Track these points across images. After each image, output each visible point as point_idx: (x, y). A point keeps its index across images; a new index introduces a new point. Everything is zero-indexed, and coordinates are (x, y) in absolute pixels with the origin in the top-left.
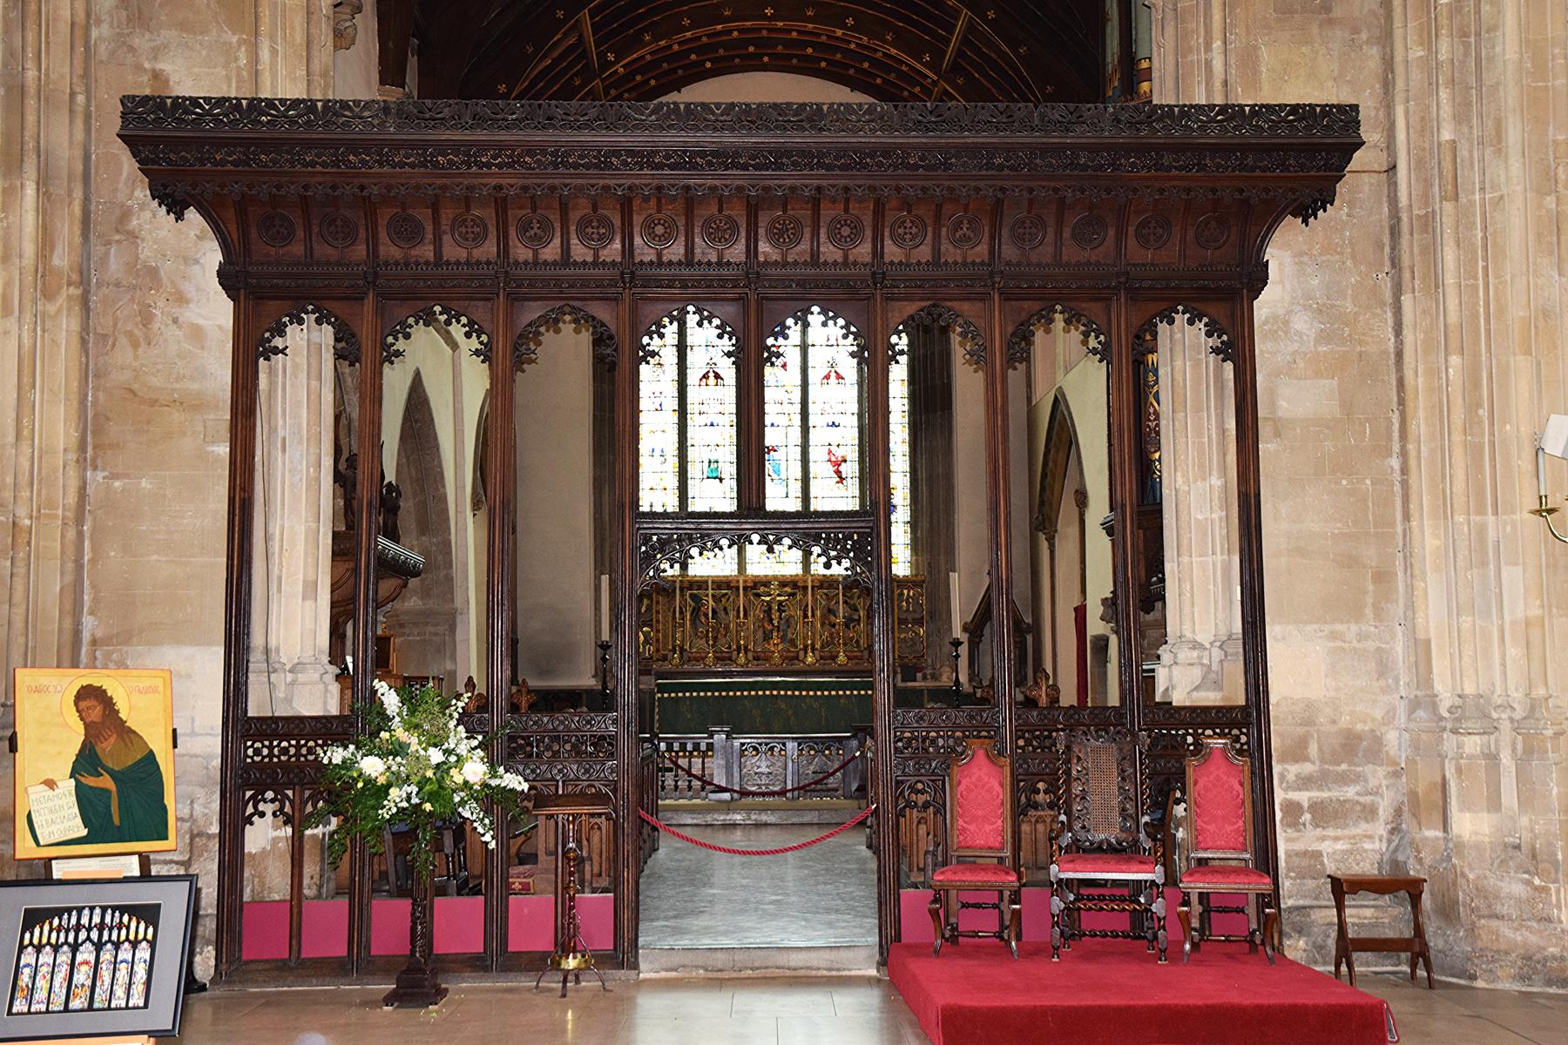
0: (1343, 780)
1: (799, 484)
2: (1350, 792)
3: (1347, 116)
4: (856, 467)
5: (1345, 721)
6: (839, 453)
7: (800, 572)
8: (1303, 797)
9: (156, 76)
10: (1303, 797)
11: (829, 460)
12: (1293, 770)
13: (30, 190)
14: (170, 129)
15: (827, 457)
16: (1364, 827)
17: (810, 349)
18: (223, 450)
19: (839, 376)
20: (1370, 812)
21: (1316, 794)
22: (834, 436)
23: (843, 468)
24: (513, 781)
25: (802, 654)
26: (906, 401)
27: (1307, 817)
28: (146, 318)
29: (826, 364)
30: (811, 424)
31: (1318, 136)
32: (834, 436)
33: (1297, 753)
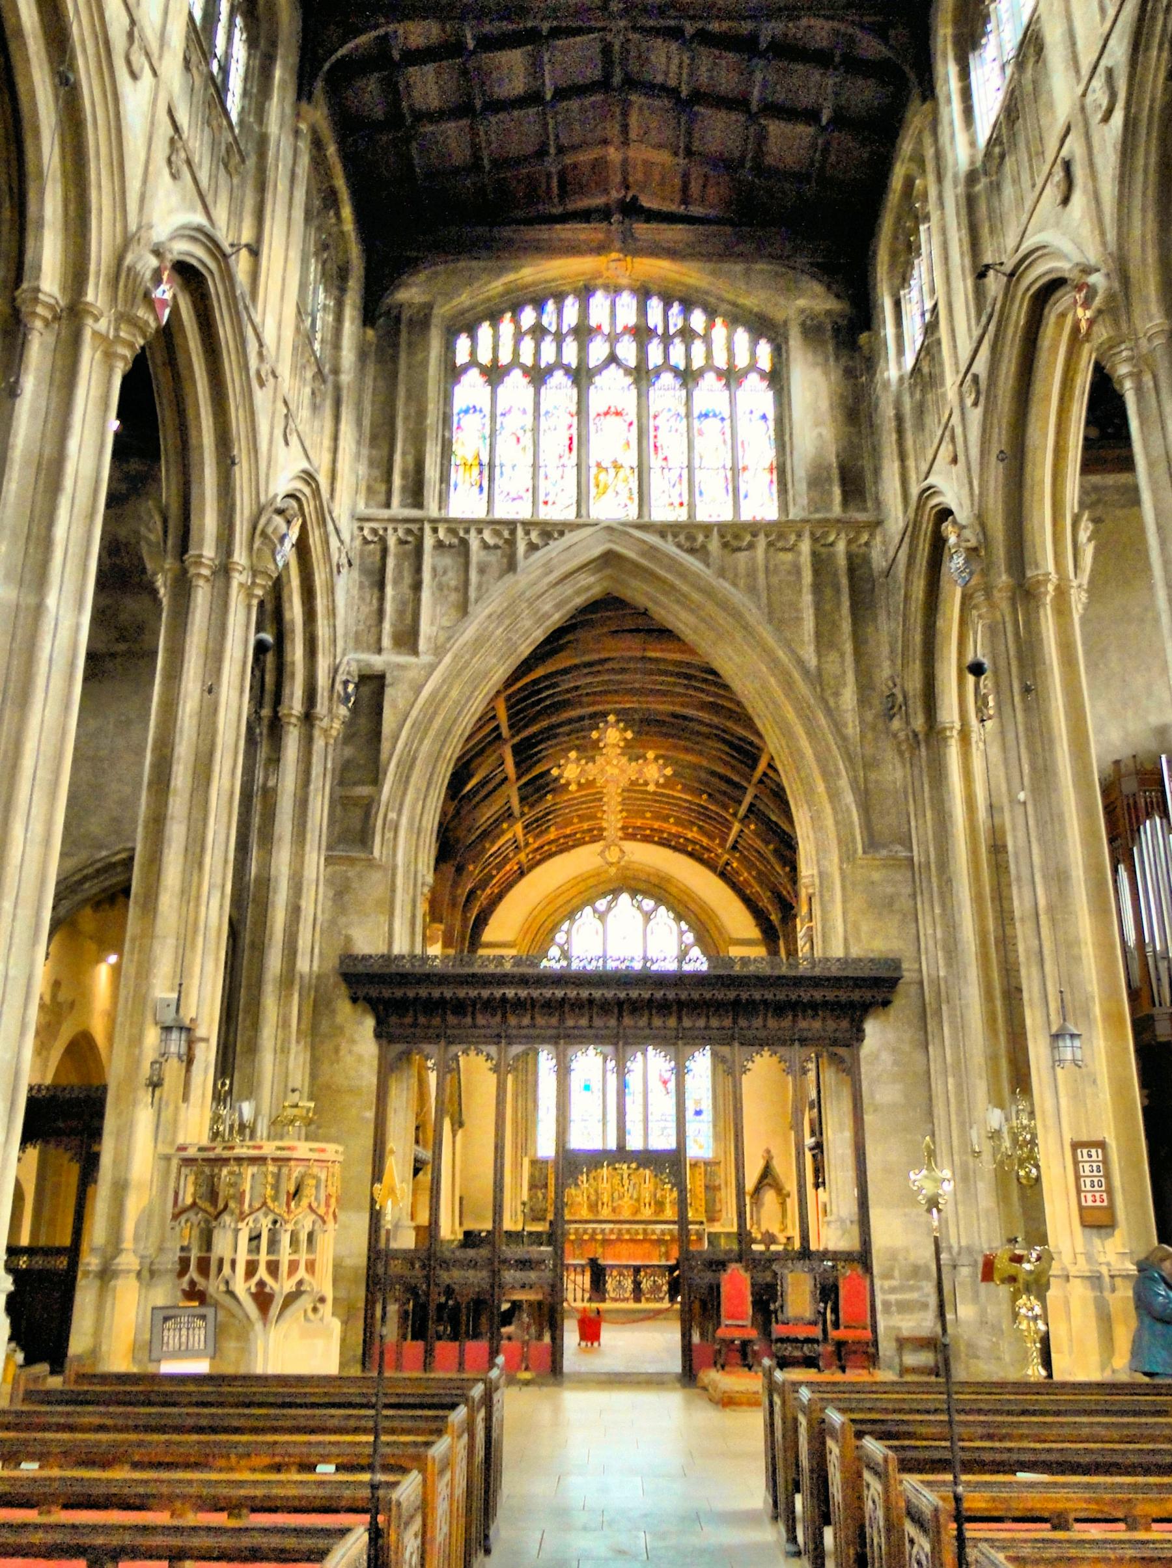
0: (912, 1289)
2: (914, 1296)
3: (896, 964)
5: (912, 1257)
8: (892, 1298)
9: (348, 939)
10: (892, 1298)
12: (887, 1284)
13: (296, 996)
14: (360, 968)
16: (921, 1315)
18: (370, 1114)
20: (925, 1306)
21: (899, 1297)
27: (894, 1309)
28: (337, 1050)
31: (884, 974)
33: (888, 1276)
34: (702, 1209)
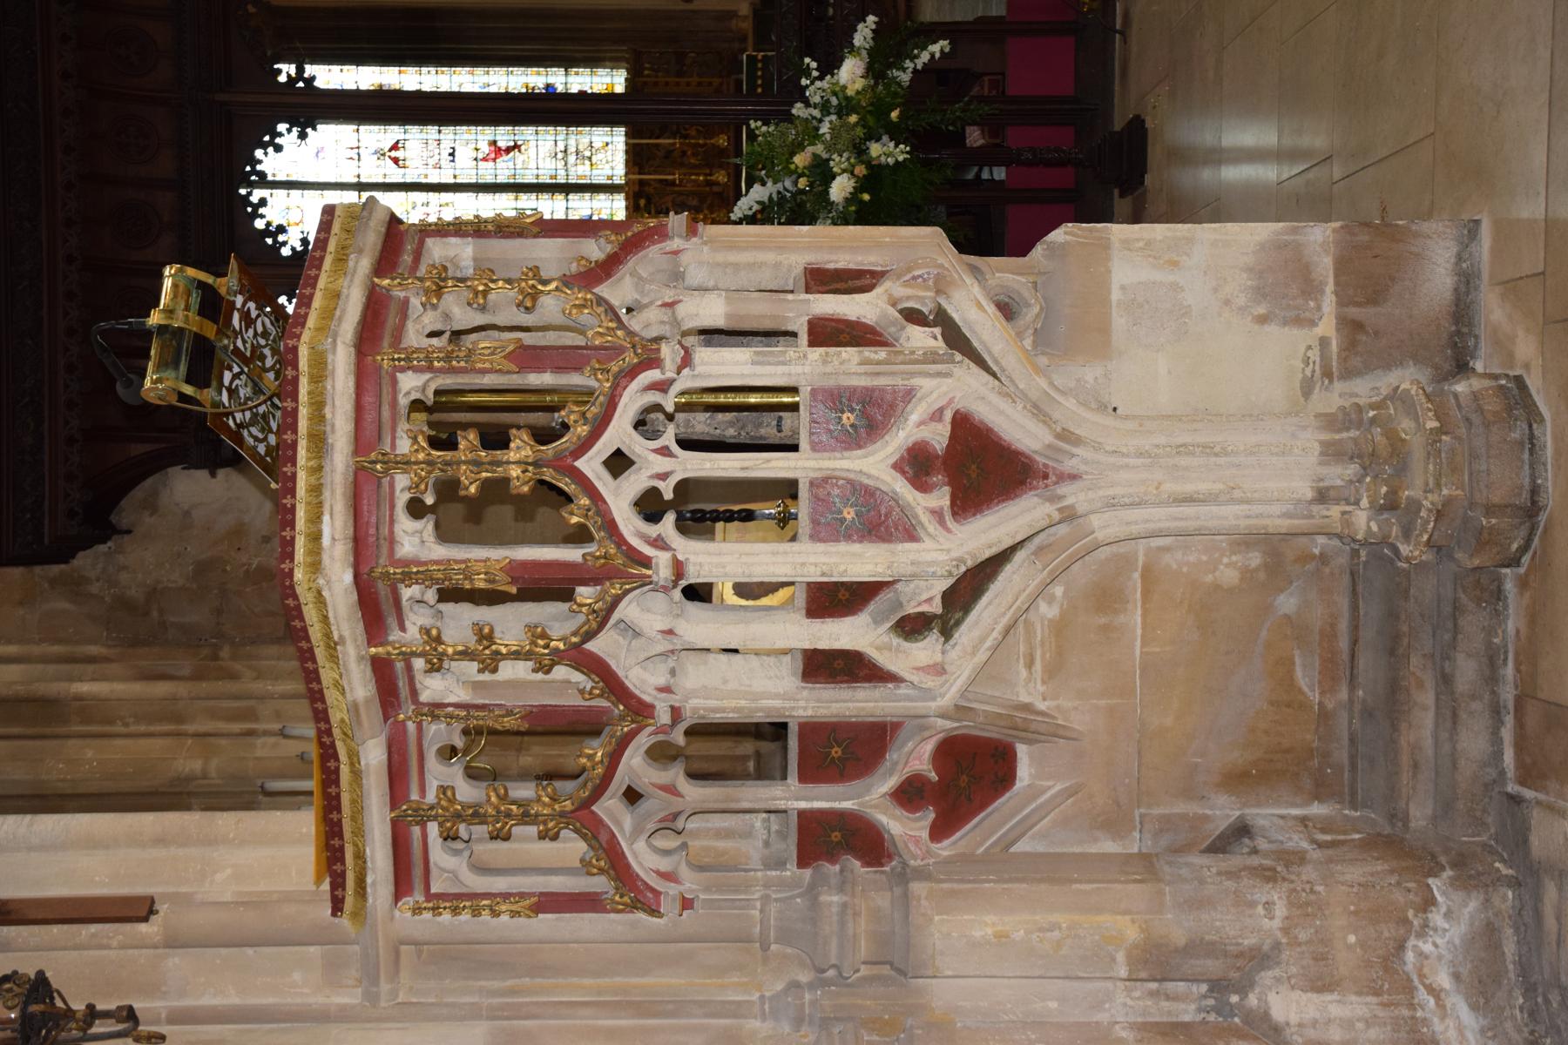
1: (523, 196)
4: (502, 129)
6: (485, 148)
7: (622, 196)
11: (494, 160)
15: (491, 164)
17: (363, 180)
19: (395, 147)
22: (465, 155)
23: (502, 144)
24: (863, 35)
25: (715, 189)
26: (424, 70)
29: (381, 162)
30: (452, 181)
32: (465, 155)
34: (716, 81)
